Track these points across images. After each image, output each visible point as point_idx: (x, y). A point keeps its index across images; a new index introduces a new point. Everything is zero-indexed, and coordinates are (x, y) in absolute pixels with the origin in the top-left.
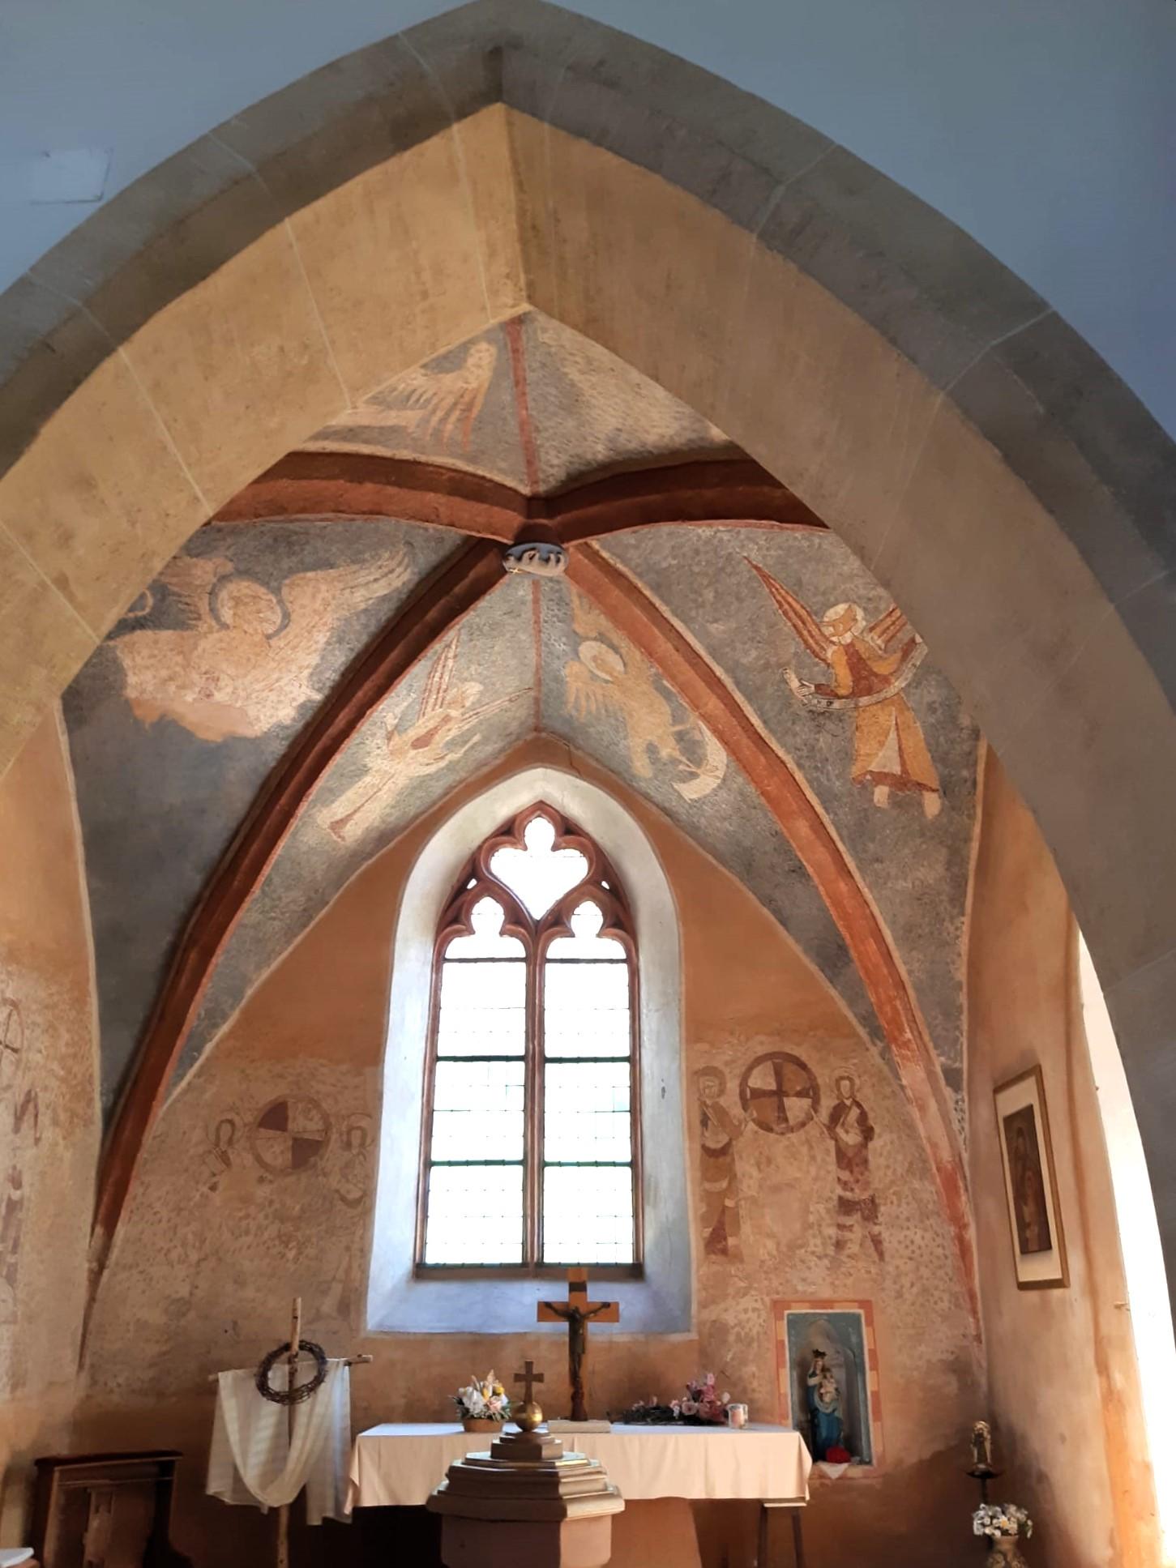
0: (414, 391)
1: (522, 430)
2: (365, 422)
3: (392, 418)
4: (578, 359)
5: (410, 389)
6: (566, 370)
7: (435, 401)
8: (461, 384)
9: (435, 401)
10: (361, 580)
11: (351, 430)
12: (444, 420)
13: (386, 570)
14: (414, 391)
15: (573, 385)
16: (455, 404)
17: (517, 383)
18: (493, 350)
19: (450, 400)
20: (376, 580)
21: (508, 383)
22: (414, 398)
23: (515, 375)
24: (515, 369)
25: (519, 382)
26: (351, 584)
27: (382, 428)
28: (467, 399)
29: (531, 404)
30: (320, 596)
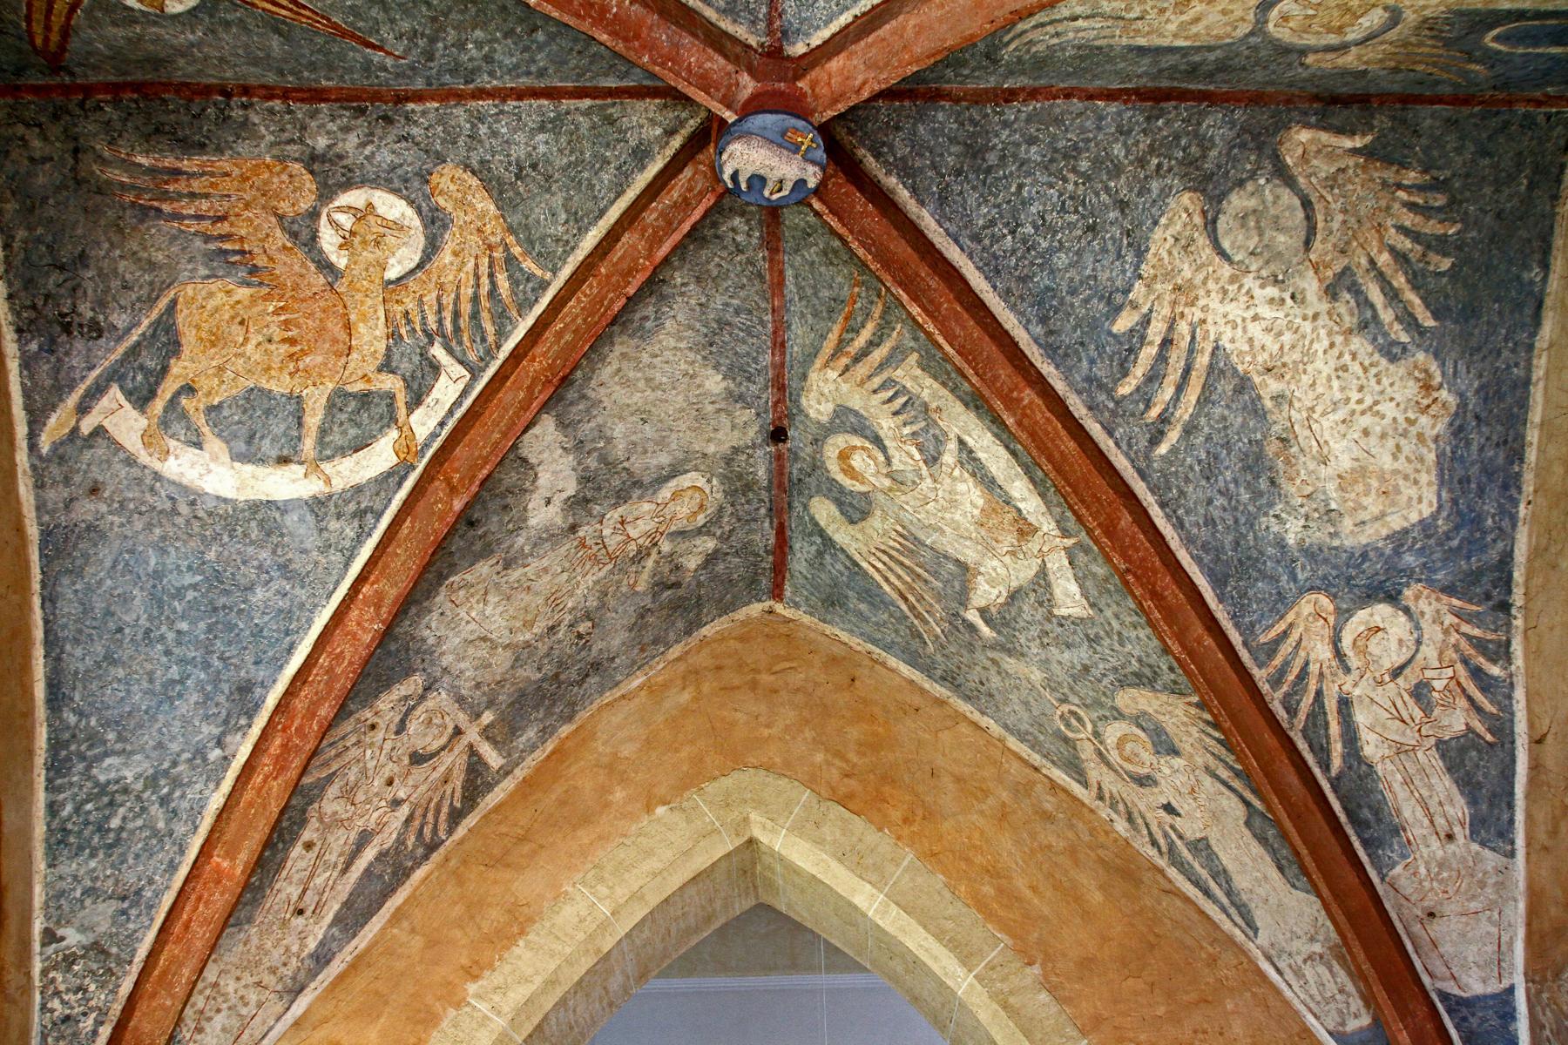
0: (896, 413)
1: (781, 272)
2: (959, 407)
3: (928, 389)
4: (710, 408)
5: (901, 417)
6: (724, 384)
7: (877, 381)
8: (845, 387)
9: (877, 381)
10: (1097, 23)
11: (977, 408)
12: (872, 345)
13: (1048, 28)
14: (896, 413)
15: (716, 367)
16: (857, 360)
17: (783, 345)
18: (803, 401)
19: (862, 370)
20: (1075, 18)
21: (795, 349)
22: (902, 400)
23: (783, 354)
24: (782, 364)
25: (780, 345)
26: (1121, 23)
27: (944, 384)
28: (845, 361)
29: (769, 318)
30: (1184, 18)
